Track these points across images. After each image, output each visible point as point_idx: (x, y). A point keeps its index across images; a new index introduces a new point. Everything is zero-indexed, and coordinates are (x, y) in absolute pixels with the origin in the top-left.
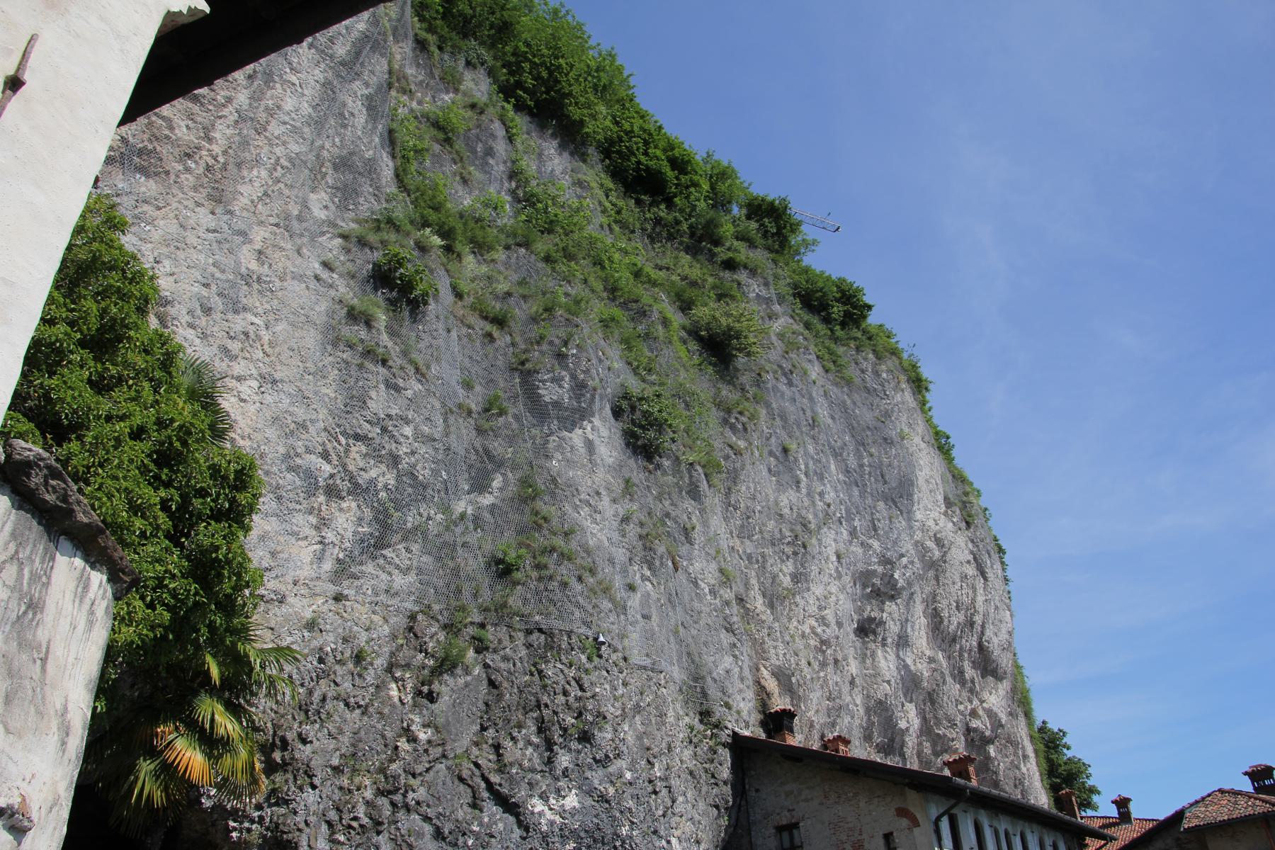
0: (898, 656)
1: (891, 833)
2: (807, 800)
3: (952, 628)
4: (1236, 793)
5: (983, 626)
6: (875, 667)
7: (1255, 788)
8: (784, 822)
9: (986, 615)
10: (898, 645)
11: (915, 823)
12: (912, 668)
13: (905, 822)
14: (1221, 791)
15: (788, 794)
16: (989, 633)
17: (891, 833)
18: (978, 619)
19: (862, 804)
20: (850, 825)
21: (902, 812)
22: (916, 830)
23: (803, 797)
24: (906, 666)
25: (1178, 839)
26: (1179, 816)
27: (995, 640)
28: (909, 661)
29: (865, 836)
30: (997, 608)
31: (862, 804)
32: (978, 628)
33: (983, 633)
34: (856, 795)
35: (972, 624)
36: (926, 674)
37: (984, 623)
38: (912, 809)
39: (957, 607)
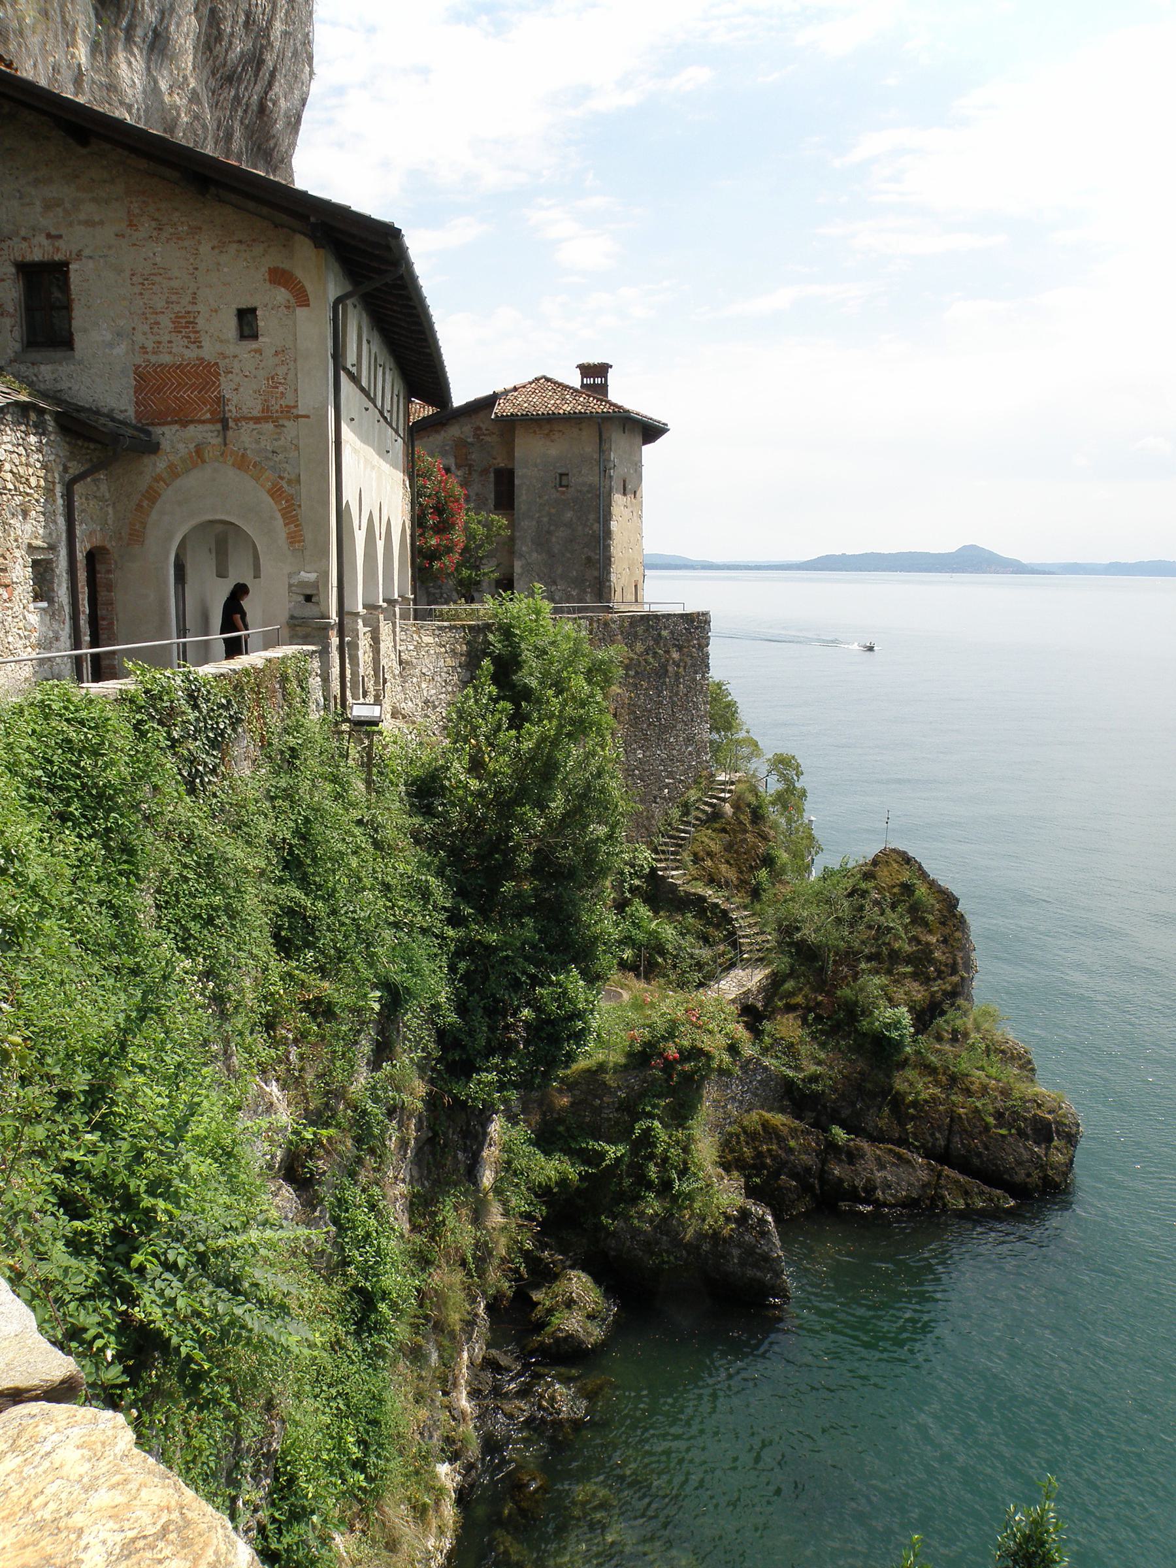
0: (148, 69)
1: (253, 311)
2: (89, 223)
3: (234, 55)
4: (566, 387)
5: (273, 75)
6: (111, 73)
7: (583, 385)
8: (37, 256)
9: (281, 56)
10: (152, 48)
11: (302, 299)
12: (167, 99)
13: (282, 295)
14: (548, 380)
15: (48, 206)
16: (276, 88)
17: (253, 311)
18: (270, 59)
19: (205, 248)
20: (175, 284)
21: (279, 277)
22: (301, 312)
23: (82, 216)
24: (156, 90)
25: (479, 428)
26: (490, 401)
27: (282, 102)
28: (163, 86)
29: (200, 307)
30: (295, 53)
31: (205, 248)
32: (265, 74)
33: (270, 85)
34: (195, 230)
35: (261, 62)
36: (185, 119)
37: (275, 68)
38: (299, 274)
39: (246, 24)
